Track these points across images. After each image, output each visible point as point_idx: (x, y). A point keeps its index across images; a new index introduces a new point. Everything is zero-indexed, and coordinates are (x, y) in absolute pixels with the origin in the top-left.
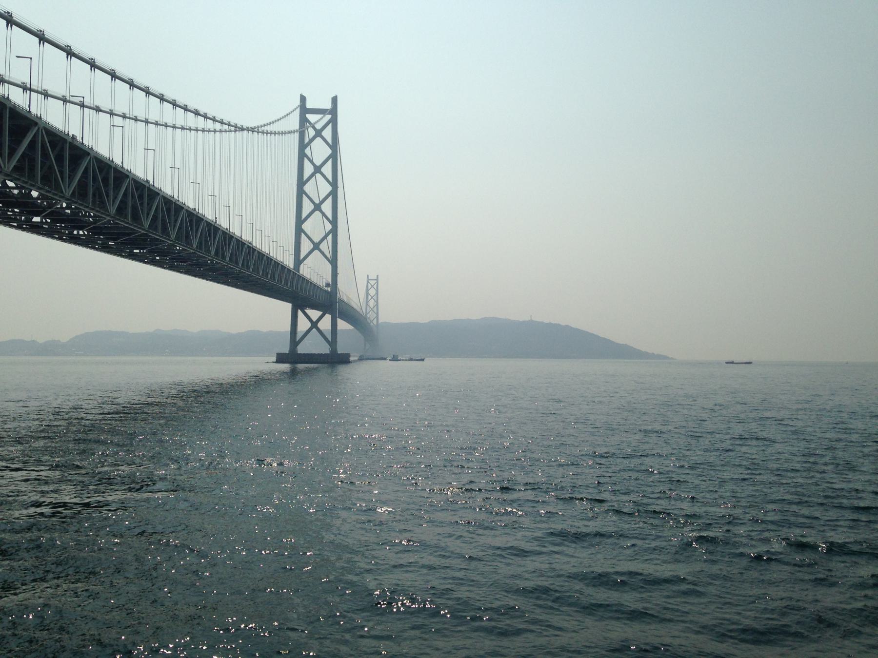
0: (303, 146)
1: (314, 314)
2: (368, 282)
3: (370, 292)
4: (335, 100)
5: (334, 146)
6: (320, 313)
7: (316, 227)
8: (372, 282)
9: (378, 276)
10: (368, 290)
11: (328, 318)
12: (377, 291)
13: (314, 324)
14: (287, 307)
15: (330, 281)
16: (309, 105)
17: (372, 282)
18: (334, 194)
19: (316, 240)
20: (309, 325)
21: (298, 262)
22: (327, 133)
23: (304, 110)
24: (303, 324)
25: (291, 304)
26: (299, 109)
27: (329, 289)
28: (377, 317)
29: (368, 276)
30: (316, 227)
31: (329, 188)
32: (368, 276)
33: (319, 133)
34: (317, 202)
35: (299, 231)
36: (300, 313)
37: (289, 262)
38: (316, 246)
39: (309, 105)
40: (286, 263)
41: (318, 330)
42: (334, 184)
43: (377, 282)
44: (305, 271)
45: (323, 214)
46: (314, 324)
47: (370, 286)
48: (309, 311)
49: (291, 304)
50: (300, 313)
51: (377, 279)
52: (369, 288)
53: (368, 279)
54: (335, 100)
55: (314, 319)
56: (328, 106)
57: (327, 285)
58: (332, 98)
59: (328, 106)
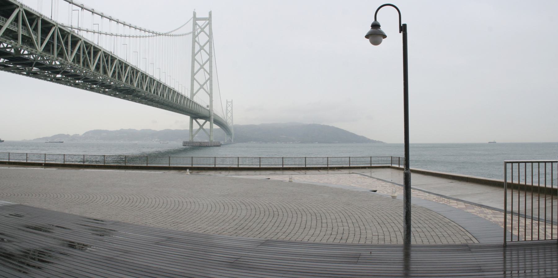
0: (195, 37)
1: (201, 121)
2: (227, 104)
3: (228, 108)
5: (210, 36)
6: (203, 121)
7: (201, 77)
8: (230, 103)
9: (232, 100)
10: (227, 107)
11: (208, 123)
12: (232, 108)
13: (201, 127)
14: (187, 118)
15: (209, 105)
16: (197, 16)
17: (230, 103)
18: (210, 60)
19: (202, 83)
20: (198, 127)
21: (193, 95)
22: (207, 30)
23: (195, 19)
24: (196, 126)
26: (193, 18)
27: (208, 109)
29: (227, 100)
30: (201, 77)
31: (208, 57)
32: (227, 100)
33: (202, 30)
34: (202, 64)
35: (193, 79)
37: (188, 94)
38: (202, 87)
39: (197, 16)
40: (186, 95)
41: (204, 129)
42: (210, 54)
43: (232, 103)
44: (196, 99)
45: (205, 70)
46: (201, 127)
47: (228, 105)
48: (199, 120)
50: (194, 121)
52: (228, 106)
53: (227, 102)
55: (201, 124)
56: (207, 16)
57: (208, 106)
58: (209, 13)
59: (207, 16)
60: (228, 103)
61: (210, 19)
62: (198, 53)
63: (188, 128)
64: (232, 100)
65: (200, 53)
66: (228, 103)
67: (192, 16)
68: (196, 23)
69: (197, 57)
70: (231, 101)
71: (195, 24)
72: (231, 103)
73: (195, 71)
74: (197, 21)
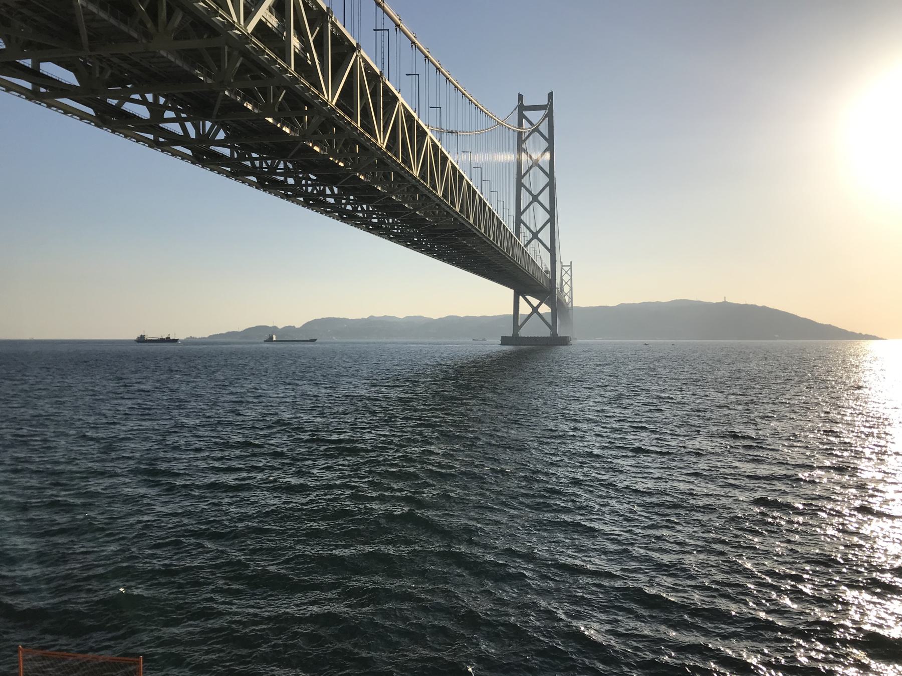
1: (535, 302)
4: (550, 96)
13: (535, 310)
14: (509, 293)
16: (525, 103)
20: (530, 310)
24: (525, 309)
25: (512, 291)
36: (521, 297)
39: (525, 103)
46: (535, 310)
49: (512, 291)
50: (521, 297)
54: (550, 96)
55: (535, 306)
61: (548, 109)
62: (525, 174)
65: (528, 174)
67: (516, 103)
69: (525, 181)
71: (521, 117)
73: (522, 208)
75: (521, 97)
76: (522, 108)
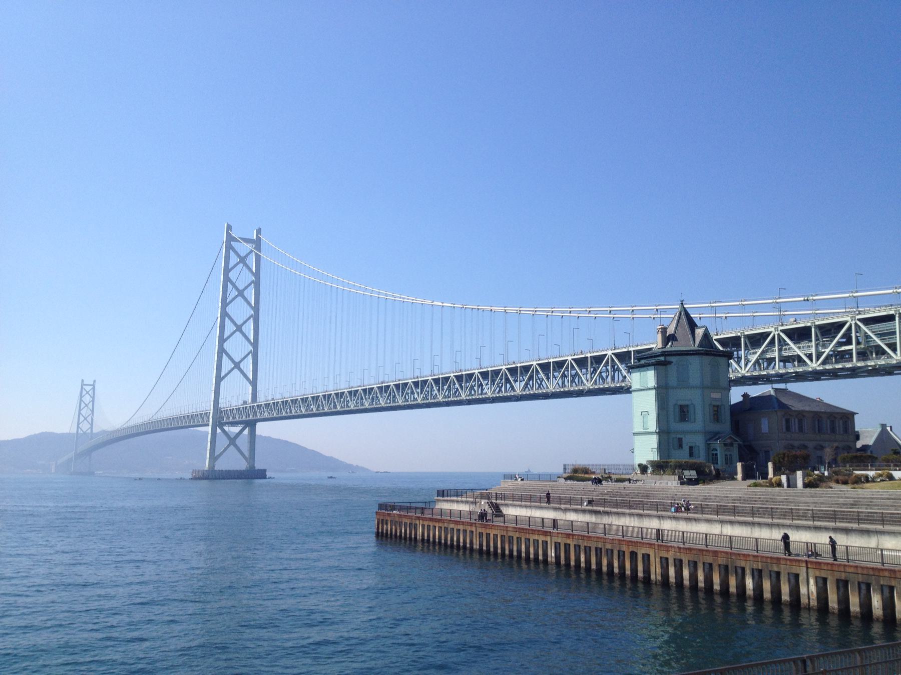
2: (82, 388)
8: (88, 388)
9: (95, 381)
28: (91, 428)
29: (83, 381)
32: (83, 381)
43: (94, 389)
51: (93, 385)
60: (84, 387)
61: (257, 243)
63: (76, 432)
64: (95, 381)
66: (84, 387)
68: (231, 245)
70: (92, 383)
71: (229, 248)
72: (92, 387)
74: (233, 243)
75: (229, 227)
76: (230, 238)
